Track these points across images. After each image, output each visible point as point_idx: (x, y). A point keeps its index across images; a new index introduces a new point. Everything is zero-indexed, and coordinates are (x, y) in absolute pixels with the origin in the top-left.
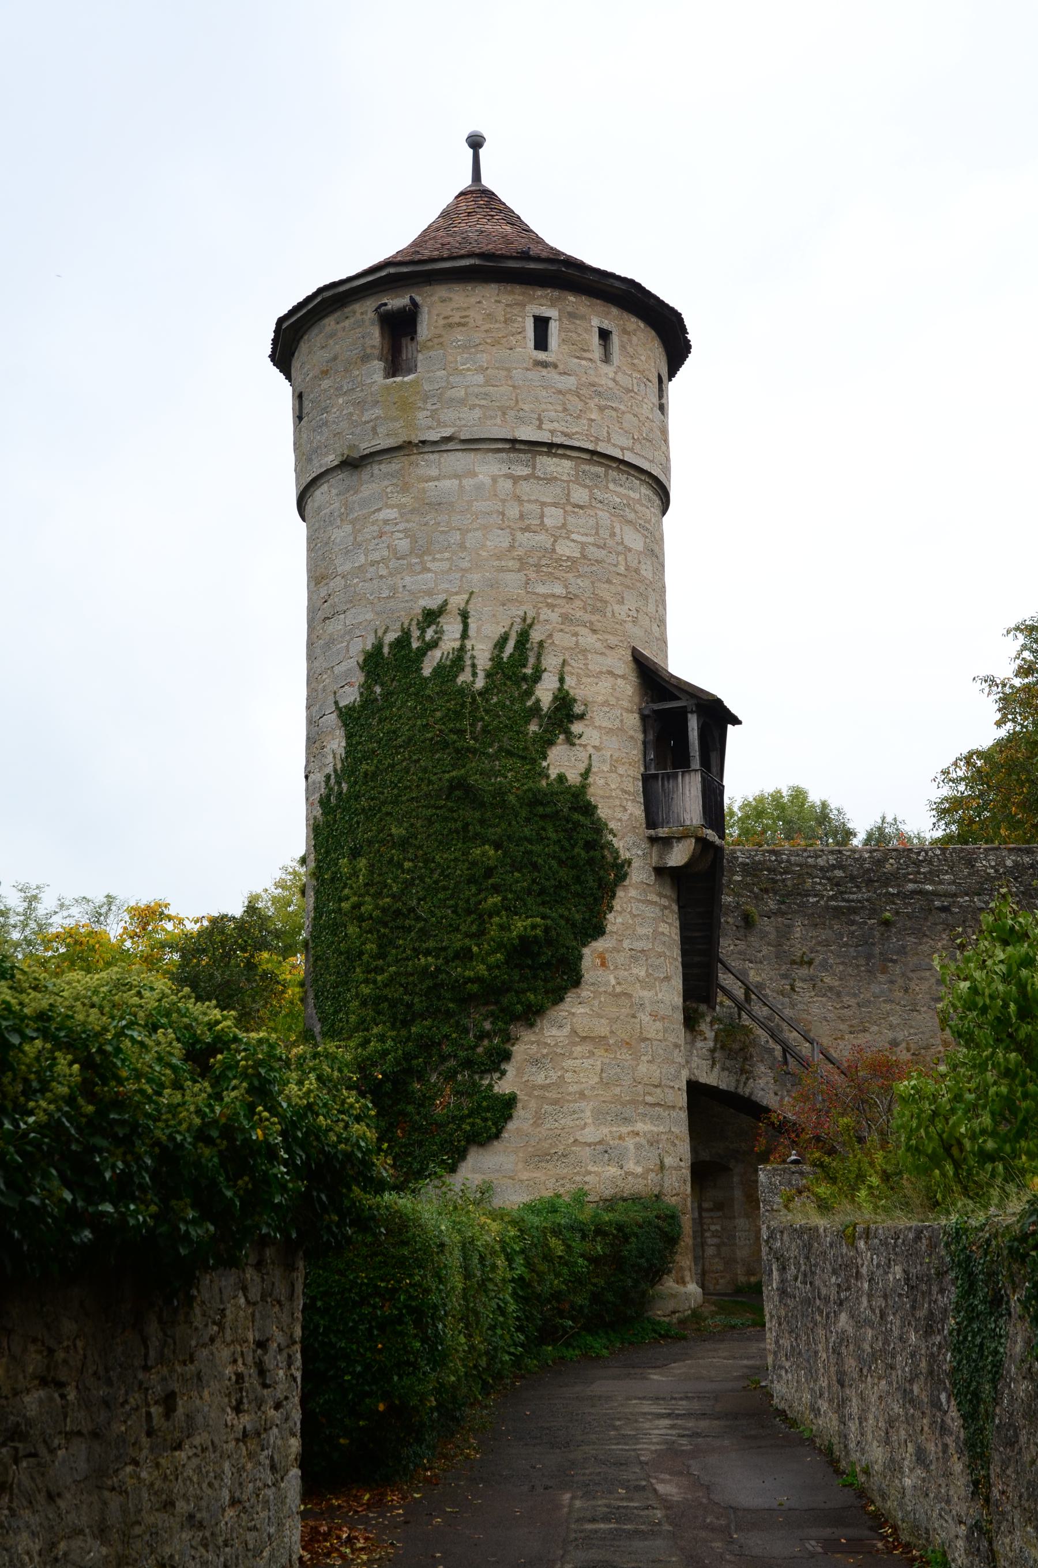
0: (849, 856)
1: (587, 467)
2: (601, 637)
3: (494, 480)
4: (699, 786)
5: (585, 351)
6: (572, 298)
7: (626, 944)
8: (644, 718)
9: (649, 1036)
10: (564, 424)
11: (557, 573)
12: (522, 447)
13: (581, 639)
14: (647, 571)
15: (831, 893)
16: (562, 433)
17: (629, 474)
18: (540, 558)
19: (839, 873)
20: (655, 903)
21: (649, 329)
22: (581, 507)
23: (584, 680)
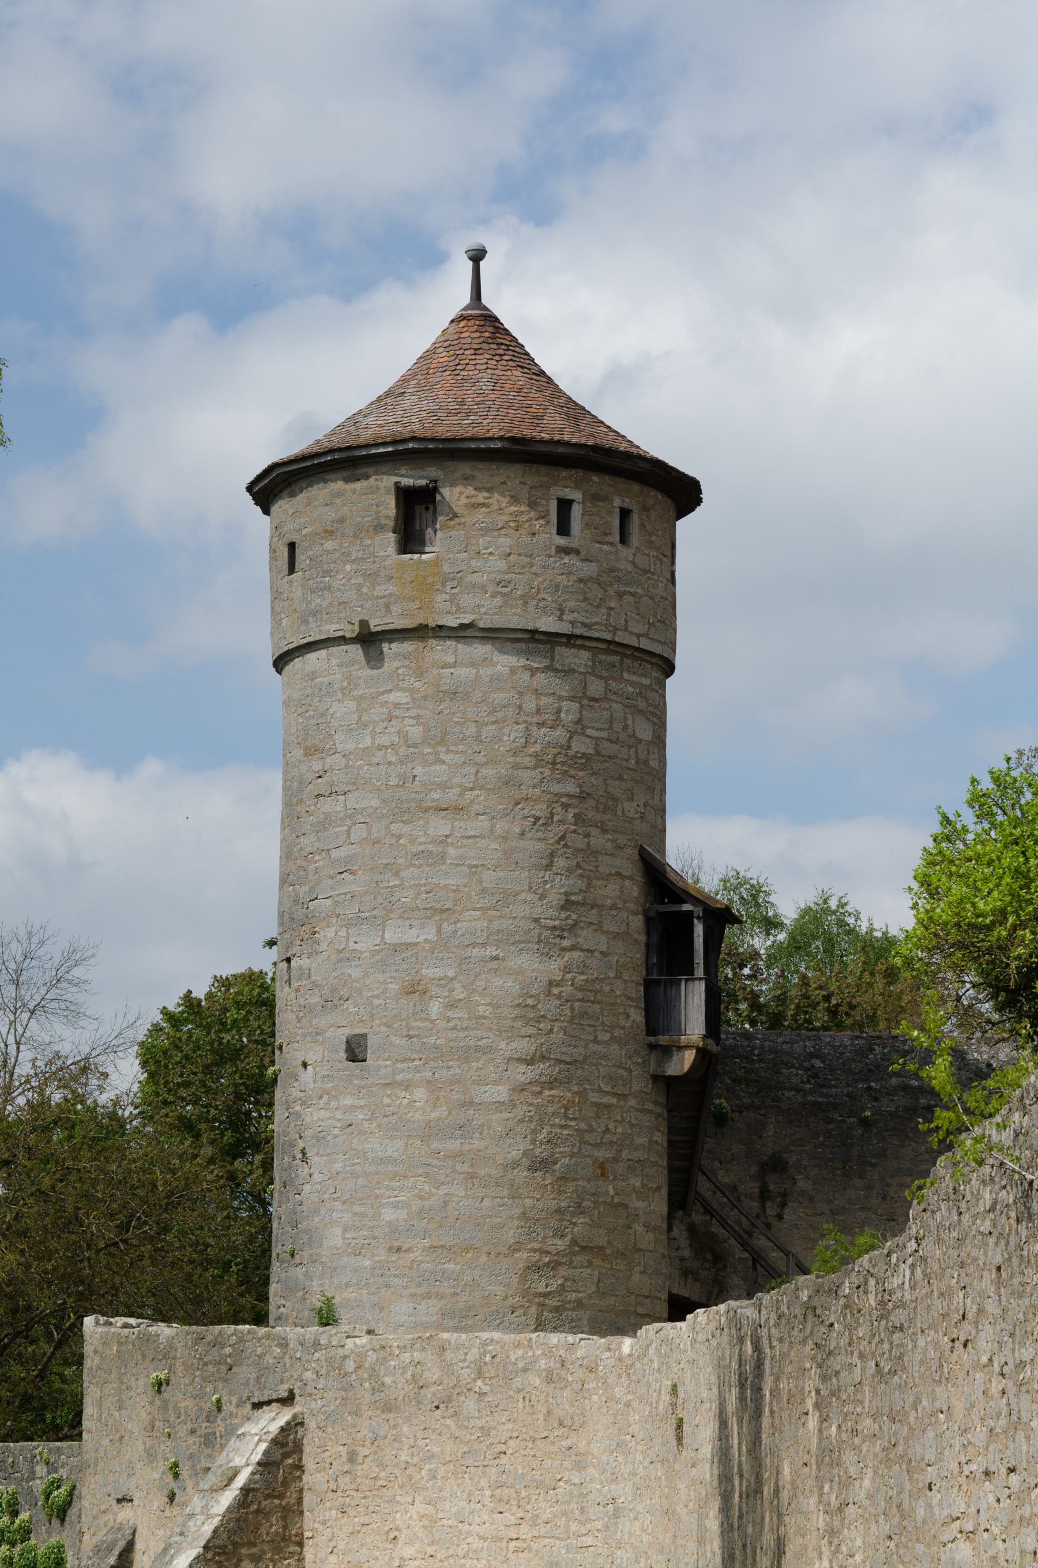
0: (829, 1043)
1: (603, 657)
2: (610, 837)
3: (513, 671)
4: (703, 995)
5: (606, 534)
6: (595, 479)
7: (625, 1154)
8: (648, 920)
9: (642, 1247)
10: (584, 614)
11: (572, 772)
12: (542, 637)
13: (593, 841)
14: (654, 764)
15: (808, 1086)
16: (582, 623)
17: (642, 660)
18: (555, 756)
19: (818, 1063)
20: (649, 1111)
21: (666, 498)
22: (596, 700)
23: (595, 882)
